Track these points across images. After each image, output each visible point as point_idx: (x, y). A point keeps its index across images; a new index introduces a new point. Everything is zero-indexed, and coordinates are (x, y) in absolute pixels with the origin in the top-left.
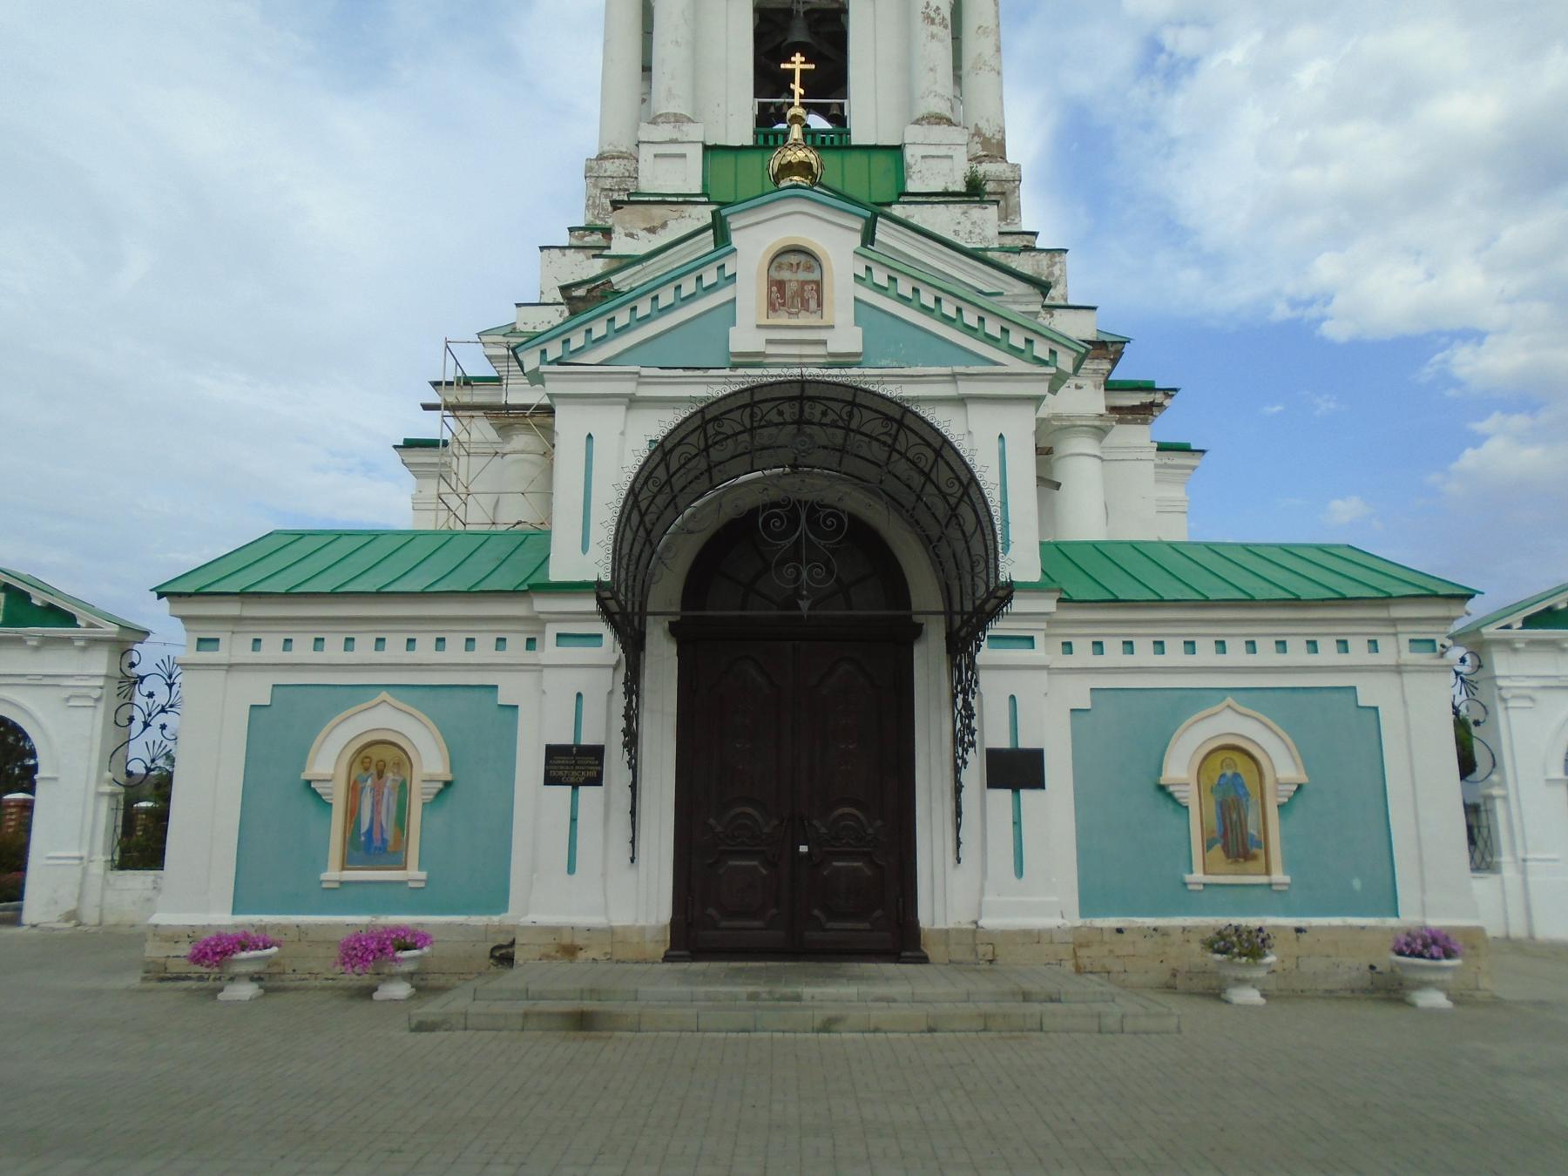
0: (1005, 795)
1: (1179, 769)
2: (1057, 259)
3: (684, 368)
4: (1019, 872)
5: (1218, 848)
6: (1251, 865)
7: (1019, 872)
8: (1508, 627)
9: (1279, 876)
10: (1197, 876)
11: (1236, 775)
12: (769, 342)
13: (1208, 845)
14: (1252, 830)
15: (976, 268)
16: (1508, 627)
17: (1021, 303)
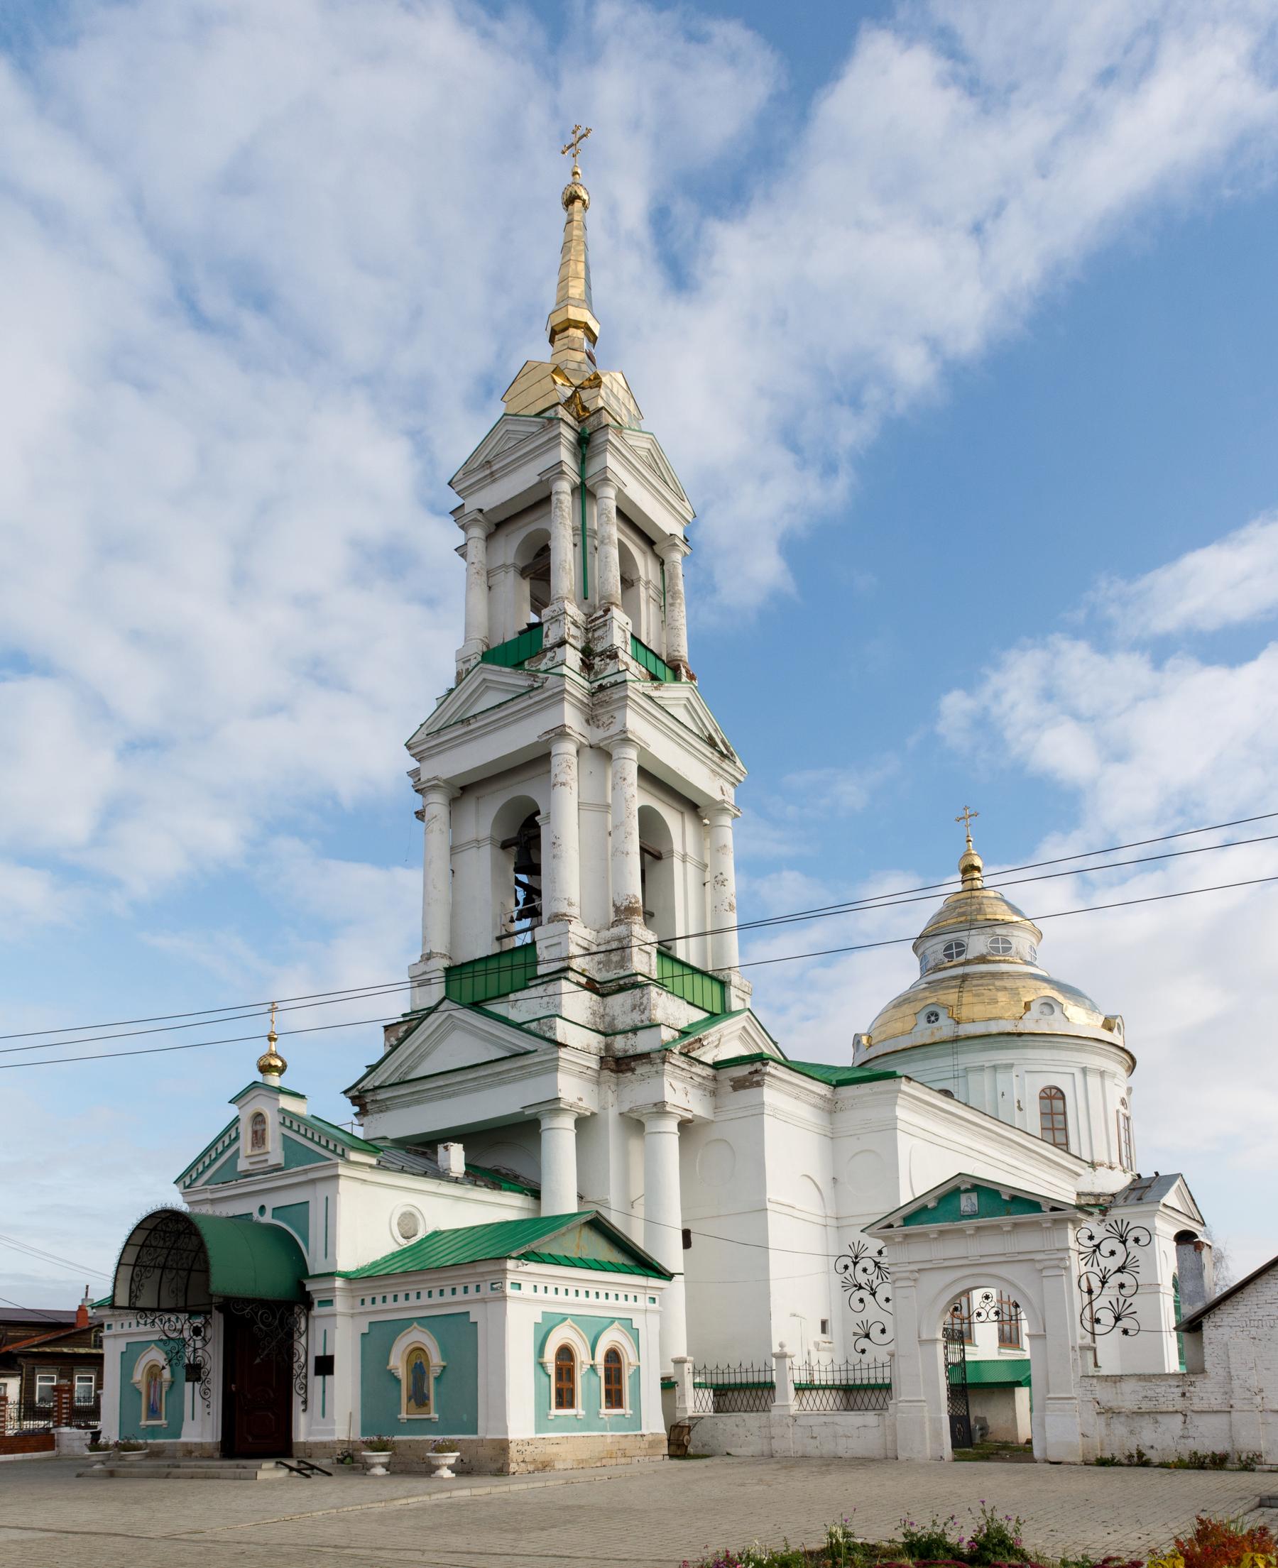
0: (320, 1378)
1: (398, 1362)
2: (645, 992)
3: (223, 1183)
4: (324, 1416)
5: (413, 1400)
6: (424, 1409)
7: (324, 1416)
8: (890, 1226)
9: (434, 1415)
10: (404, 1415)
11: (421, 1363)
12: (251, 1163)
13: (409, 1399)
14: (426, 1392)
15: (523, 1036)
16: (890, 1226)
17: (548, 1054)
